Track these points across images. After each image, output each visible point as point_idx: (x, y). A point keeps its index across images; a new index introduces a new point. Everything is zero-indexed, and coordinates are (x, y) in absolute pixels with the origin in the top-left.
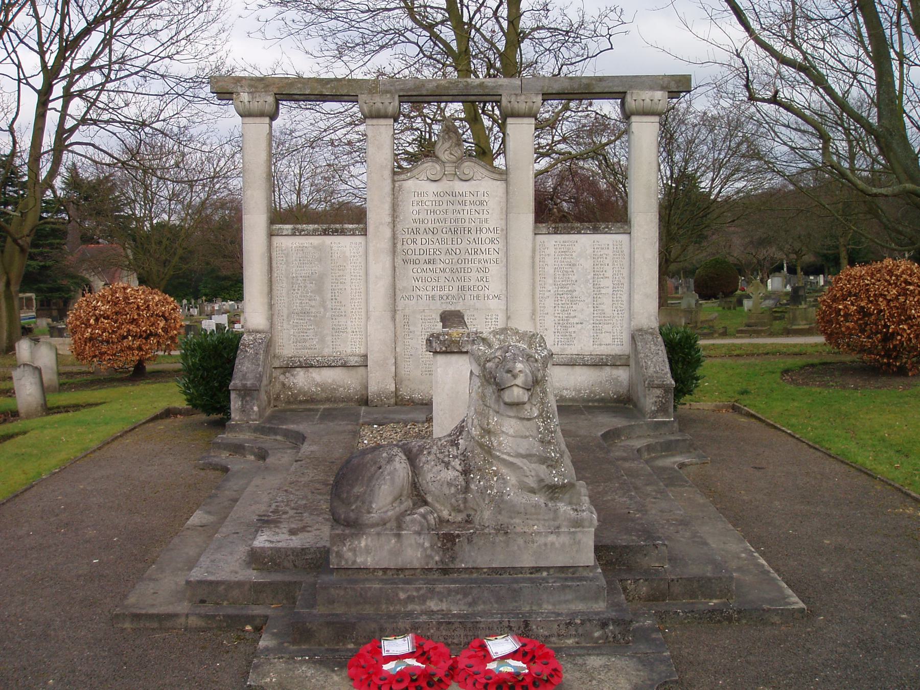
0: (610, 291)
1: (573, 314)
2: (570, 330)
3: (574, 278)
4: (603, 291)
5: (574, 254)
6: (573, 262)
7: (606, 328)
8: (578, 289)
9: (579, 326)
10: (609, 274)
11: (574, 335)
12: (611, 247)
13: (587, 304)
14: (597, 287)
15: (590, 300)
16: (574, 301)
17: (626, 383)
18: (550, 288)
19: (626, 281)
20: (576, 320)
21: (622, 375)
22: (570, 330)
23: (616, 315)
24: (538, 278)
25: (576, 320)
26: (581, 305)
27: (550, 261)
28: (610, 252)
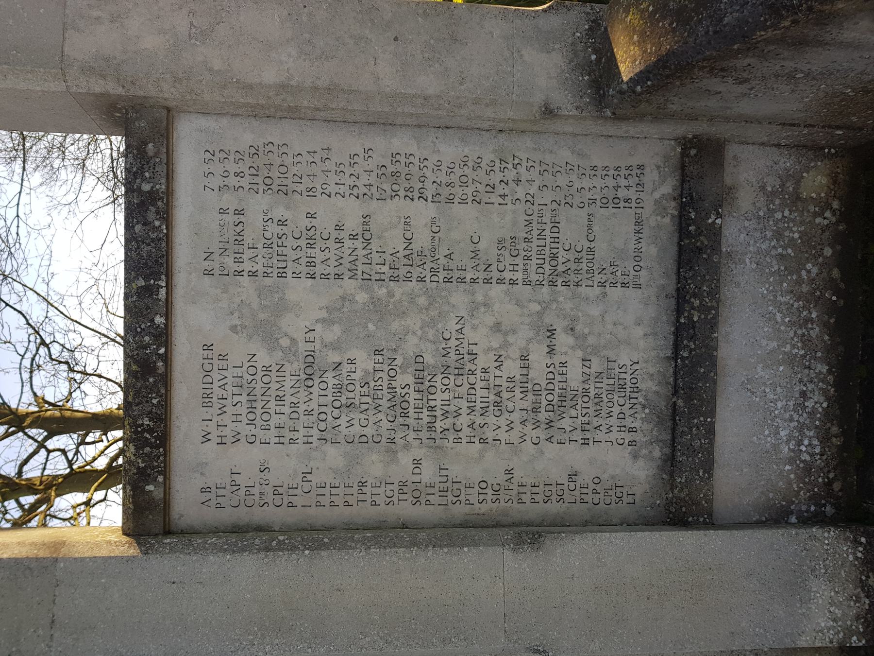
0: (422, 213)
1: (512, 368)
2: (575, 374)
3: (364, 362)
4: (422, 240)
5: (263, 358)
6: (297, 366)
7: (572, 232)
8: (412, 345)
9: (563, 340)
10: (351, 213)
11: (596, 365)
12: (229, 200)
13: (474, 308)
14: (410, 263)
15: (459, 299)
16: (459, 363)
17: (787, 162)
18: (405, 460)
19: (383, 145)
20: (538, 357)
21: (752, 170)
22: (575, 374)
23: (520, 193)
24: (362, 512)
25: (538, 357)
26: (479, 336)
27: (285, 465)
28: (258, 205)
